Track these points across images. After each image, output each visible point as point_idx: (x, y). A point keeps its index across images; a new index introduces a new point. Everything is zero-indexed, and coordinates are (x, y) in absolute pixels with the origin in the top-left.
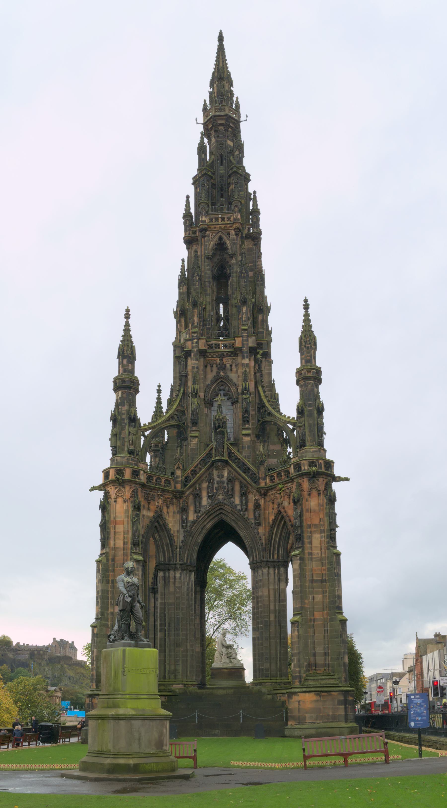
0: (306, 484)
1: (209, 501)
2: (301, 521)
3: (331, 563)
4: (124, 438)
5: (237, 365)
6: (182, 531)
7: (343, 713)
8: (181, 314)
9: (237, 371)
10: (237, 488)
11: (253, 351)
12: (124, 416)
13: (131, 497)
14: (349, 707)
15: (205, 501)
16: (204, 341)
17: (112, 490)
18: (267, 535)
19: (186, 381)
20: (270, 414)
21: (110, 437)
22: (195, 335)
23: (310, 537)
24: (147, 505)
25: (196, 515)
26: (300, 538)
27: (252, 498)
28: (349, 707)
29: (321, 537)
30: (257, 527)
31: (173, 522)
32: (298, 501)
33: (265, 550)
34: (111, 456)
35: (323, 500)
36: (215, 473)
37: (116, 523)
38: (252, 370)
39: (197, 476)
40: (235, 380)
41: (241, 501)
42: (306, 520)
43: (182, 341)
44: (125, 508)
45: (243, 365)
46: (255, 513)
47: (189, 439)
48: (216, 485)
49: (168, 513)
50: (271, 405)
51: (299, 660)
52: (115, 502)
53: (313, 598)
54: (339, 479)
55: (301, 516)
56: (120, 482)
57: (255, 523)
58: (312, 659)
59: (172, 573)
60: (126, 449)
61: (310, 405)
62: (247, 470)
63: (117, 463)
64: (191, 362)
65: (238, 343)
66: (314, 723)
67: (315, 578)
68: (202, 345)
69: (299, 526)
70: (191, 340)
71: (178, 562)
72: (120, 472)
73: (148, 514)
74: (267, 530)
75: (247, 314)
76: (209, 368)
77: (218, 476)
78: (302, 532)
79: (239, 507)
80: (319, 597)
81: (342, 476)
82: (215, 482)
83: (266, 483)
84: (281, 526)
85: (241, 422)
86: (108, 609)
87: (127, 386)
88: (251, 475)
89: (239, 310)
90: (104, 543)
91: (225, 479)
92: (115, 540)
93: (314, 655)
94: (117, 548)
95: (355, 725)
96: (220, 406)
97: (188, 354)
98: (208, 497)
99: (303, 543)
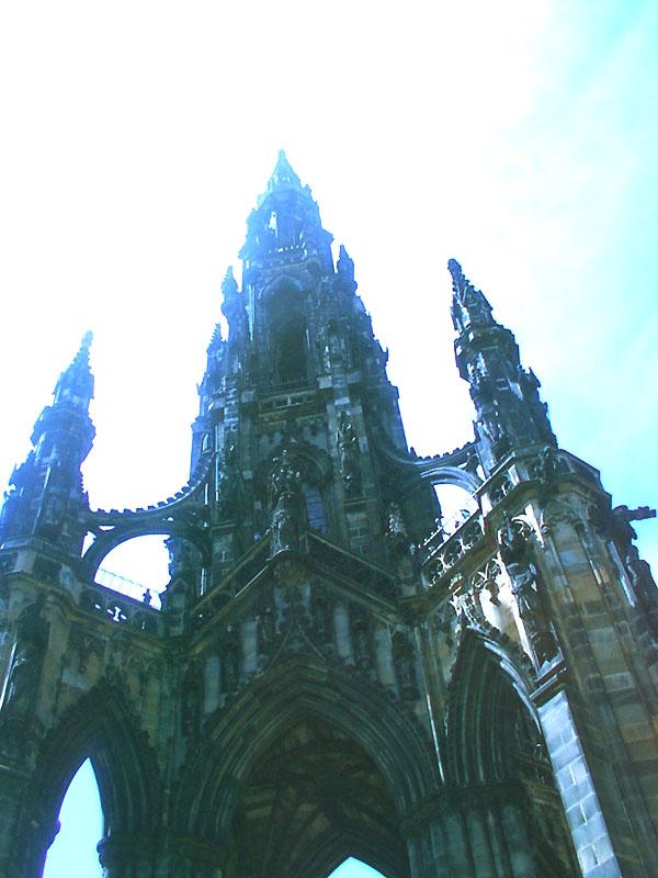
10: (341, 620)
15: (251, 662)
24: (75, 660)
25: (224, 696)
27: (384, 637)
29: (620, 631)
30: (408, 702)
41: (355, 647)
42: (557, 596)
48: (281, 619)
57: (403, 692)
62: (364, 576)
71: (165, 824)
73: (79, 682)
77: (287, 599)
79: (350, 661)
81: (632, 507)
82: (280, 613)
83: (420, 588)
91: (305, 603)
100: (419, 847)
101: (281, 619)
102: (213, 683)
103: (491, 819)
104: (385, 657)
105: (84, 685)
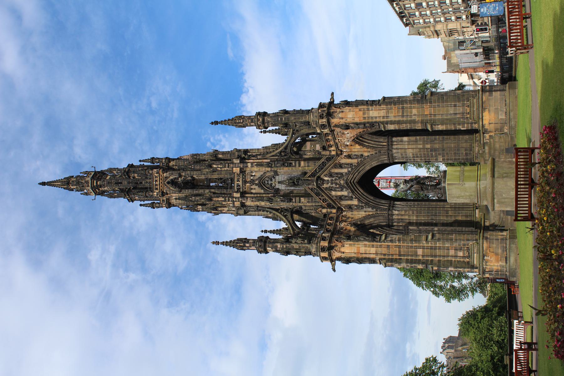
0: (335, 121)
1: (345, 189)
2: (360, 124)
3: (390, 103)
4: (299, 247)
5: (252, 172)
6: (365, 209)
7: (499, 92)
8: (216, 210)
9: (255, 172)
10: (336, 171)
11: (243, 160)
12: (285, 247)
13: (340, 242)
14: (494, 89)
15: (345, 193)
16: (235, 194)
17: (336, 255)
18: (369, 150)
19: (262, 207)
20: (286, 148)
21: (298, 256)
22: (230, 199)
23: (372, 118)
26: (372, 125)
27: (344, 161)
28: (494, 89)
31: (359, 215)
32: (347, 126)
33: (380, 152)
34: (312, 256)
35: (347, 109)
36: (325, 186)
38: (255, 161)
39: (327, 198)
40: (262, 173)
41: (345, 168)
43: (234, 209)
44: (348, 246)
45: (252, 166)
46: (354, 158)
47: (301, 204)
48: (334, 185)
49: (352, 218)
50: (280, 147)
51: (459, 124)
52: (343, 253)
53: (415, 115)
54: (332, 98)
55: (357, 124)
56: (330, 248)
58: (458, 116)
59: (394, 217)
60: (307, 245)
61: (281, 119)
62: (324, 164)
63: (317, 251)
64: (249, 203)
65: (237, 170)
66: (506, 112)
67: (401, 114)
68: (238, 195)
69: (365, 125)
70: (234, 202)
72: (323, 249)
74: (366, 150)
75: (218, 164)
76: (253, 191)
77: (328, 183)
78: (368, 123)
80: (414, 111)
81: (330, 97)
82: (331, 186)
83: (333, 150)
84: (364, 140)
85: (290, 168)
86: (420, 260)
87: (263, 244)
88: (327, 161)
89: (215, 171)
90: (372, 261)
91: (330, 179)
93: (456, 114)
94: (376, 252)
95: (507, 85)
96: (279, 182)
97: (243, 205)
98: (342, 190)
99: (376, 122)
100: (396, 159)
101: (334, 185)
102: (349, 202)
103: (395, 143)
105: (353, 229)
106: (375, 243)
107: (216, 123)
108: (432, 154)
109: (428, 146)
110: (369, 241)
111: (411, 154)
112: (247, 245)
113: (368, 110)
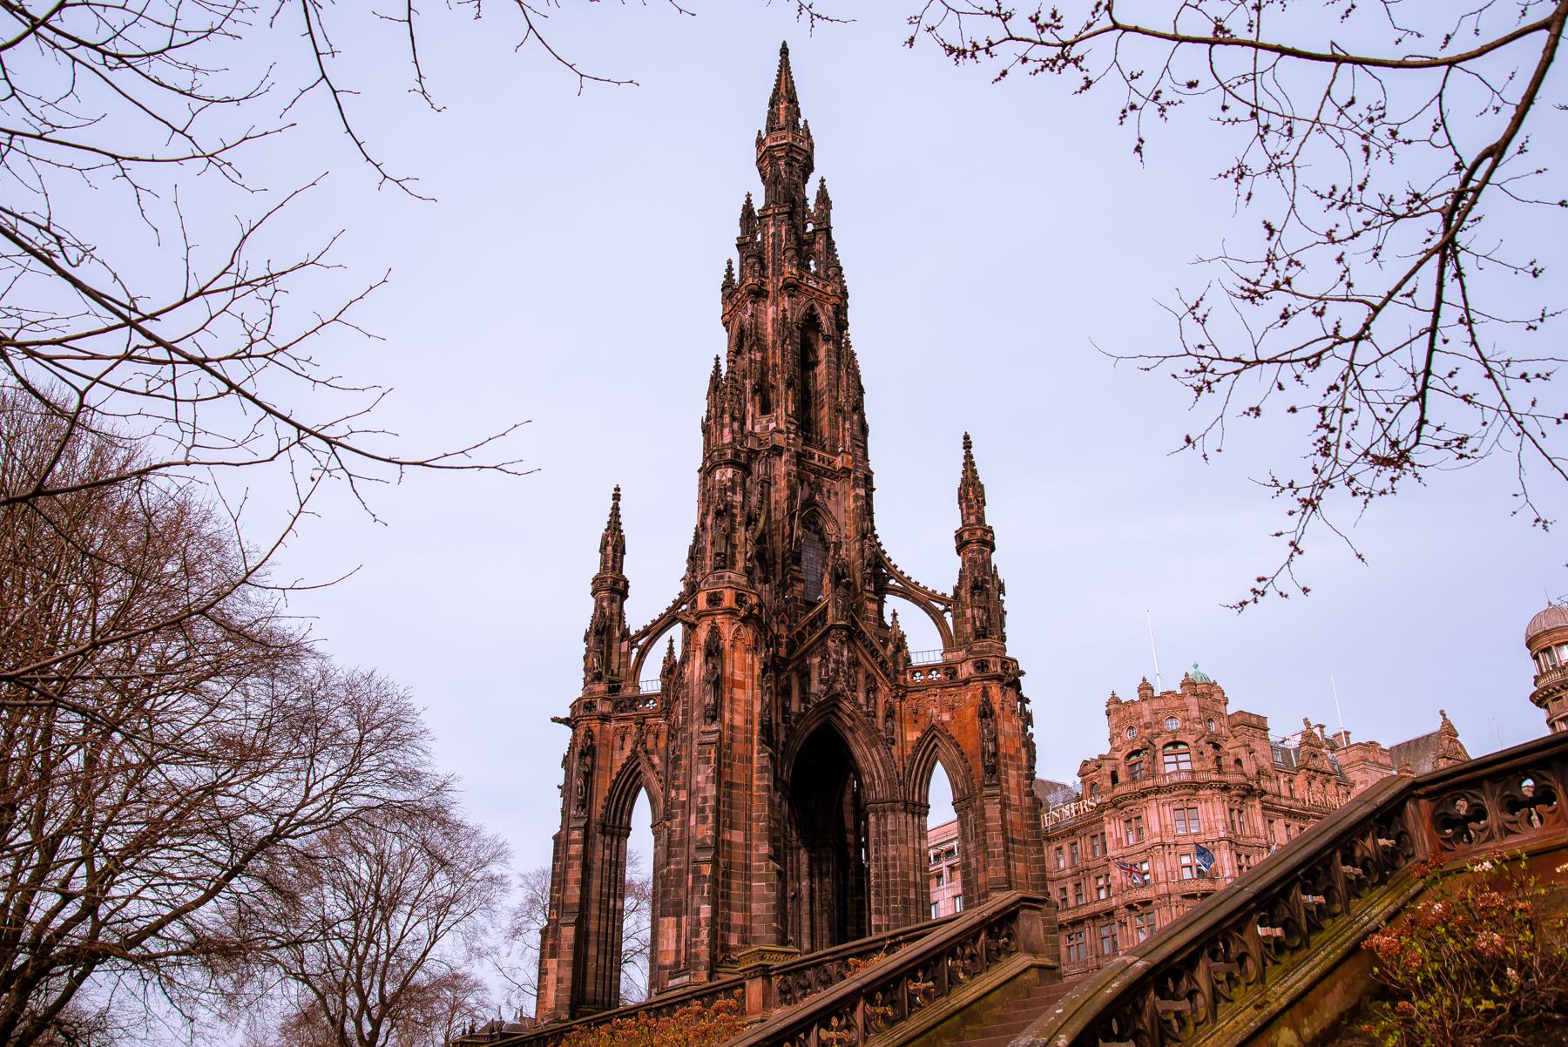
0: (995, 691)
15: (816, 687)
27: (881, 700)
29: (1019, 776)
37: (735, 684)
48: (832, 665)
60: (740, 564)
92: (732, 711)
97: (777, 451)
98: (821, 681)
99: (999, 779)
102: (795, 693)
104: (881, 714)
106: (757, 728)
107: (967, 445)
108: (895, 901)
109: (912, 896)
110: (762, 715)
111: (891, 853)
112: (736, 425)
113: (1019, 768)
